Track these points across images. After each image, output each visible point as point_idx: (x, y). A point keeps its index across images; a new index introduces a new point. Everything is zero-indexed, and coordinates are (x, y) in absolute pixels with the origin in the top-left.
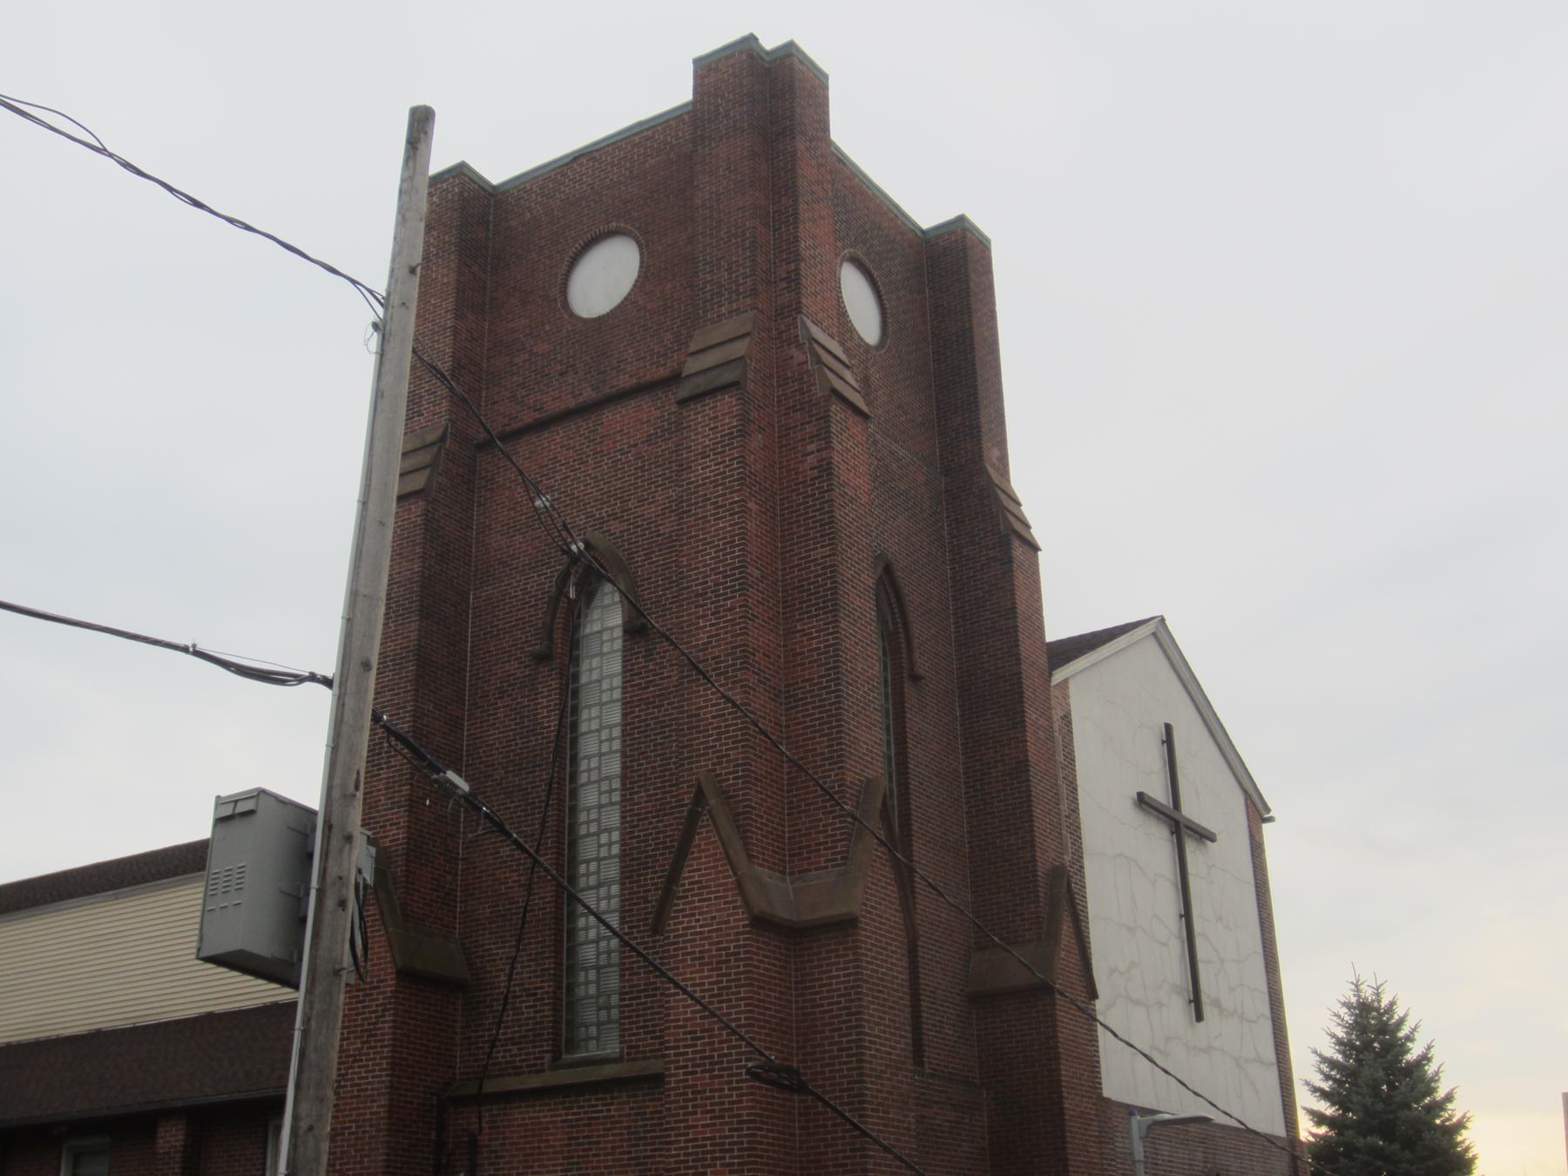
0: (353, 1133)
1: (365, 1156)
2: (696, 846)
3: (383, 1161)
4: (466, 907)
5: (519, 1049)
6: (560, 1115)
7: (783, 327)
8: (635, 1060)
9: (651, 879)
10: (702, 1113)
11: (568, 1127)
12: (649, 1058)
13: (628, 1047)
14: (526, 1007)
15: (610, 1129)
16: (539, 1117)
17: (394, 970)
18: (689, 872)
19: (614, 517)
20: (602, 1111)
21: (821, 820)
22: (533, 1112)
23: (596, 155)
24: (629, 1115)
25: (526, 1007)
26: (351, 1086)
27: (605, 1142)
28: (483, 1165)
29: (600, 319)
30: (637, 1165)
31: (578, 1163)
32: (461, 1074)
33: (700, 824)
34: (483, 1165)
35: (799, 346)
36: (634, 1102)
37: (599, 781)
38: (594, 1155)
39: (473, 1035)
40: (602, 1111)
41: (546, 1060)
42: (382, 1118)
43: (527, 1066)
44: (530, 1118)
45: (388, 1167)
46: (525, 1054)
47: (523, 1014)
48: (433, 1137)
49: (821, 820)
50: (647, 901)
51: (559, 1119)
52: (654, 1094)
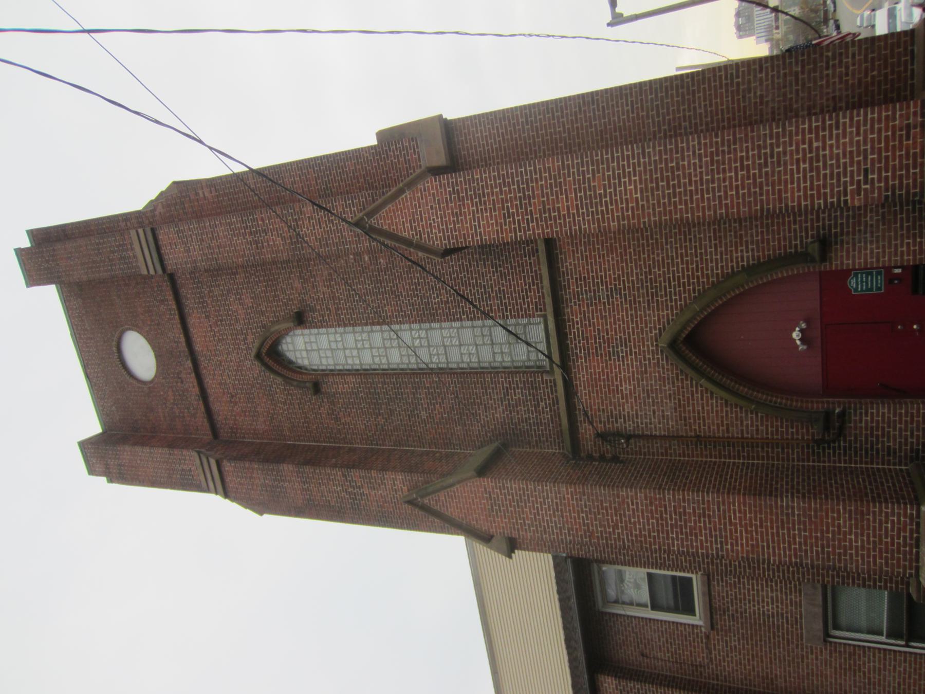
0: (587, 516)
1: (602, 505)
2: (389, 227)
3: (604, 490)
4: (457, 445)
5: (542, 401)
6: (582, 363)
7: (147, 221)
8: (544, 305)
9: (434, 299)
10: (558, 203)
11: (589, 356)
12: (543, 293)
13: (537, 311)
14: (515, 396)
15: (589, 321)
16: (584, 381)
17: (478, 479)
18: (405, 232)
19: (245, 339)
20: (578, 329)
21: (392, 161)
22: (581, 386)
23: (86, 362)
24: (579, 305)
25: (515, 396)
26: (555, 517)
27: (598, 325)
28: (617, 428)
29: (158, 357)
30: (612, 298)
31: (613, 347)
32: (560, 449)
33: (376, 226)
34: (617, 428)
35: (155, 210)
36: (571, 302)
37: (385, 348)
38: (608, 334)
39: (534, 439)
40: (578, 329)
41: (548, 378)
42: (575, 489)
43: (552, 394)
44: (585, 389)
45: (609, 486)
46: (545, 396)
47: (519, 398)
48: (597, 463)
49: (392, 161)
50: (447, 302)
51: (584, 364)
52: (565, 285)
